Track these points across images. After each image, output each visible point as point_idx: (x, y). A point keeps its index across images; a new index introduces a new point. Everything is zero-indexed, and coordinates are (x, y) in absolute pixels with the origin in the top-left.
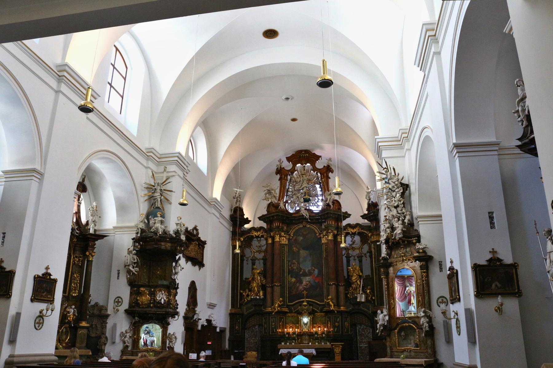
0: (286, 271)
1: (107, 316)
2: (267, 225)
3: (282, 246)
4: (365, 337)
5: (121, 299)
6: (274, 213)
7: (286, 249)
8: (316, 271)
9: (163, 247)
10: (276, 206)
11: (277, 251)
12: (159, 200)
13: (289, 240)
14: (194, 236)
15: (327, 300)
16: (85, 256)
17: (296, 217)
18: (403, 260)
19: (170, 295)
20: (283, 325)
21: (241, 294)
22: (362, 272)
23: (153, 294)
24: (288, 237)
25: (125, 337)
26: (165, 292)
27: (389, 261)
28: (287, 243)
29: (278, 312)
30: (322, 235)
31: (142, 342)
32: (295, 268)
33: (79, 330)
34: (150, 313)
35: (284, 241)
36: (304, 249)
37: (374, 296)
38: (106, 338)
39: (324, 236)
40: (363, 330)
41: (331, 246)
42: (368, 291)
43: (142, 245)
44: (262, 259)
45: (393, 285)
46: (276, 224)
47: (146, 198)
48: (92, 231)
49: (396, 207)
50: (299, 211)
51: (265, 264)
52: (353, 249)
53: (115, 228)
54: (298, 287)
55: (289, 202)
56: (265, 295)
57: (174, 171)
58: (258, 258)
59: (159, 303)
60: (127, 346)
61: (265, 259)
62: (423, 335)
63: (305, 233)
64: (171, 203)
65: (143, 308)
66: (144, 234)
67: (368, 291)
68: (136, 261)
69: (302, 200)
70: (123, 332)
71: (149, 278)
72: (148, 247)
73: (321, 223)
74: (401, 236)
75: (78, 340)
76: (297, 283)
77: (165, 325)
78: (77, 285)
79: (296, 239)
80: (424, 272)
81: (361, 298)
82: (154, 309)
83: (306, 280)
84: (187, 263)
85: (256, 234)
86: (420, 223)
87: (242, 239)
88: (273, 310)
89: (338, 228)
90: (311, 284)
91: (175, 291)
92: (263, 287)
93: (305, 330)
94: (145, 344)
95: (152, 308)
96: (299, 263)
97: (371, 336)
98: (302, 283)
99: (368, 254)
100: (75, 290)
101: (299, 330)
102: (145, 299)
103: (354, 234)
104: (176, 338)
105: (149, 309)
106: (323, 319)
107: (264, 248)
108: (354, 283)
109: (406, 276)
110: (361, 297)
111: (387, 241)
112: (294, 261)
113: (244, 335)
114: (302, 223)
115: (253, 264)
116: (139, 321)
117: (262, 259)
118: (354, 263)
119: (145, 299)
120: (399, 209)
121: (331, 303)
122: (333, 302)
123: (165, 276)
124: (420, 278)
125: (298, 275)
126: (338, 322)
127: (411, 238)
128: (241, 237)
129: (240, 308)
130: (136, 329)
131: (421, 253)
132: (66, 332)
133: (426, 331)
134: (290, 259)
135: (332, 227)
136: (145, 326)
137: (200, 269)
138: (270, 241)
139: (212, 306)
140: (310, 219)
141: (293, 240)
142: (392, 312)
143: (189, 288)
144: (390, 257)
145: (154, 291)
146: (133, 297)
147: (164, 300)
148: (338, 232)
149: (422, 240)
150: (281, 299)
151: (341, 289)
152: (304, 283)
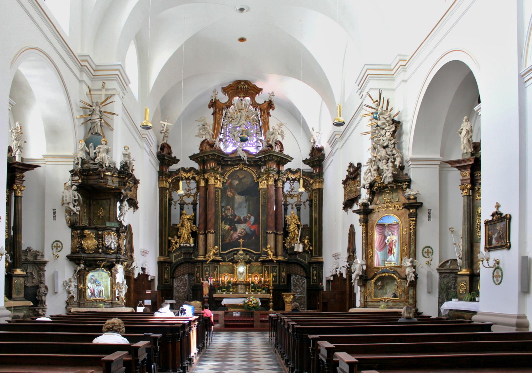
0: (219, 217)
2: (200, 165)
3: (217, 189)
4: (299, 287)
6: (209, 152)
7: (220, 192)
8: (252, 219)
10: (212, 145)
11: (212, 196)
13: (223, 183)
15: (267, 249)
17: (231, 158)
18: (387, 207)
20: (217, 274)
21: (169, 241)
22: (300, 221)
23: (100, 238)
24: (222, 179)
25: (69, 287)
27: (370, 207)
28: (221, 186)
29: (213, 261)
30: (260, 180)
31: (88, 292)
32: (229, 214)
35: (219, 185)
36: (240, 194)
37: (312, 246)
39: (262, 180)
40: (298, 280)
41: (272, 191)
42: (306, 241)
44: (192, 204)
45: (373, 233)
46: (211, 165)
49: (384, 147)
50: (235, 152)
51: (195, 210)
52: (292, 196)
54: (232, 234)
55: (223, 140)
56: (196, 242)
58: (187, 202)
60: (73, 297)
61: (194, 204)
62: (407, 285)
63: (241, 177)
65: (89, 253)
66: (86, 165)
67: (306, 241)
69: (239, 139)
70: (66, 281)
71: (90, 219)
73: (259, 167)
74: (391, 180)
76: (231, 230)
79: (230, 183)
80: (413, 221)
81: (299, 248)
82: (102, 255)
83: (241, 228)
85: (185, 175)
86: (411, 166)
87: (170, 180)
88: (207, 258)
89: (279, 172)
90: (247, 232)
92: (194, 234)
93: (241, 279)
94: (93, 294)
96: (233, 210)
97: (306, 286)
98: (236, 231)
99: (308, 202)
101: (234, 280)
103: (294, 180)
105: (97, 255)
106: (260, 268)
107: (194, 192)
108: (291, 232)
109: (386, 224)
110: (298, 247)
111: (372, 185)
112: (228, 207)
113: (173, 284)
114: (237, 165)
115: (182, 209)
116: (85, 269)
117: (192, 204)
118: (292, 212)
119: (90, 243)
120: (388, 150)
121: (270, 252)
122: (272, 252)
123: (109, 217)
124: (408, 226)
125: (233, 222)
126: (276, 272)
127: (401, 183)
128: (169, 178)
129: (168, 256)
130: (81, 277)
131: (413, 199)
133: (411, 282)
134: (223, 204)
135: (273, 170)
136: (90, 274)
137: (134, 212)
138: (202, 184)
139: (144, 253)
140: (248, 161)
141: (227, 184)
142: (369, 261)
144: (371, 204)
145: (102, 234)
146: (76, 241)
148: (279, 177)
149: (412, 186)
150: (217, 247)
151: (280, 238)
152: (239, 231)
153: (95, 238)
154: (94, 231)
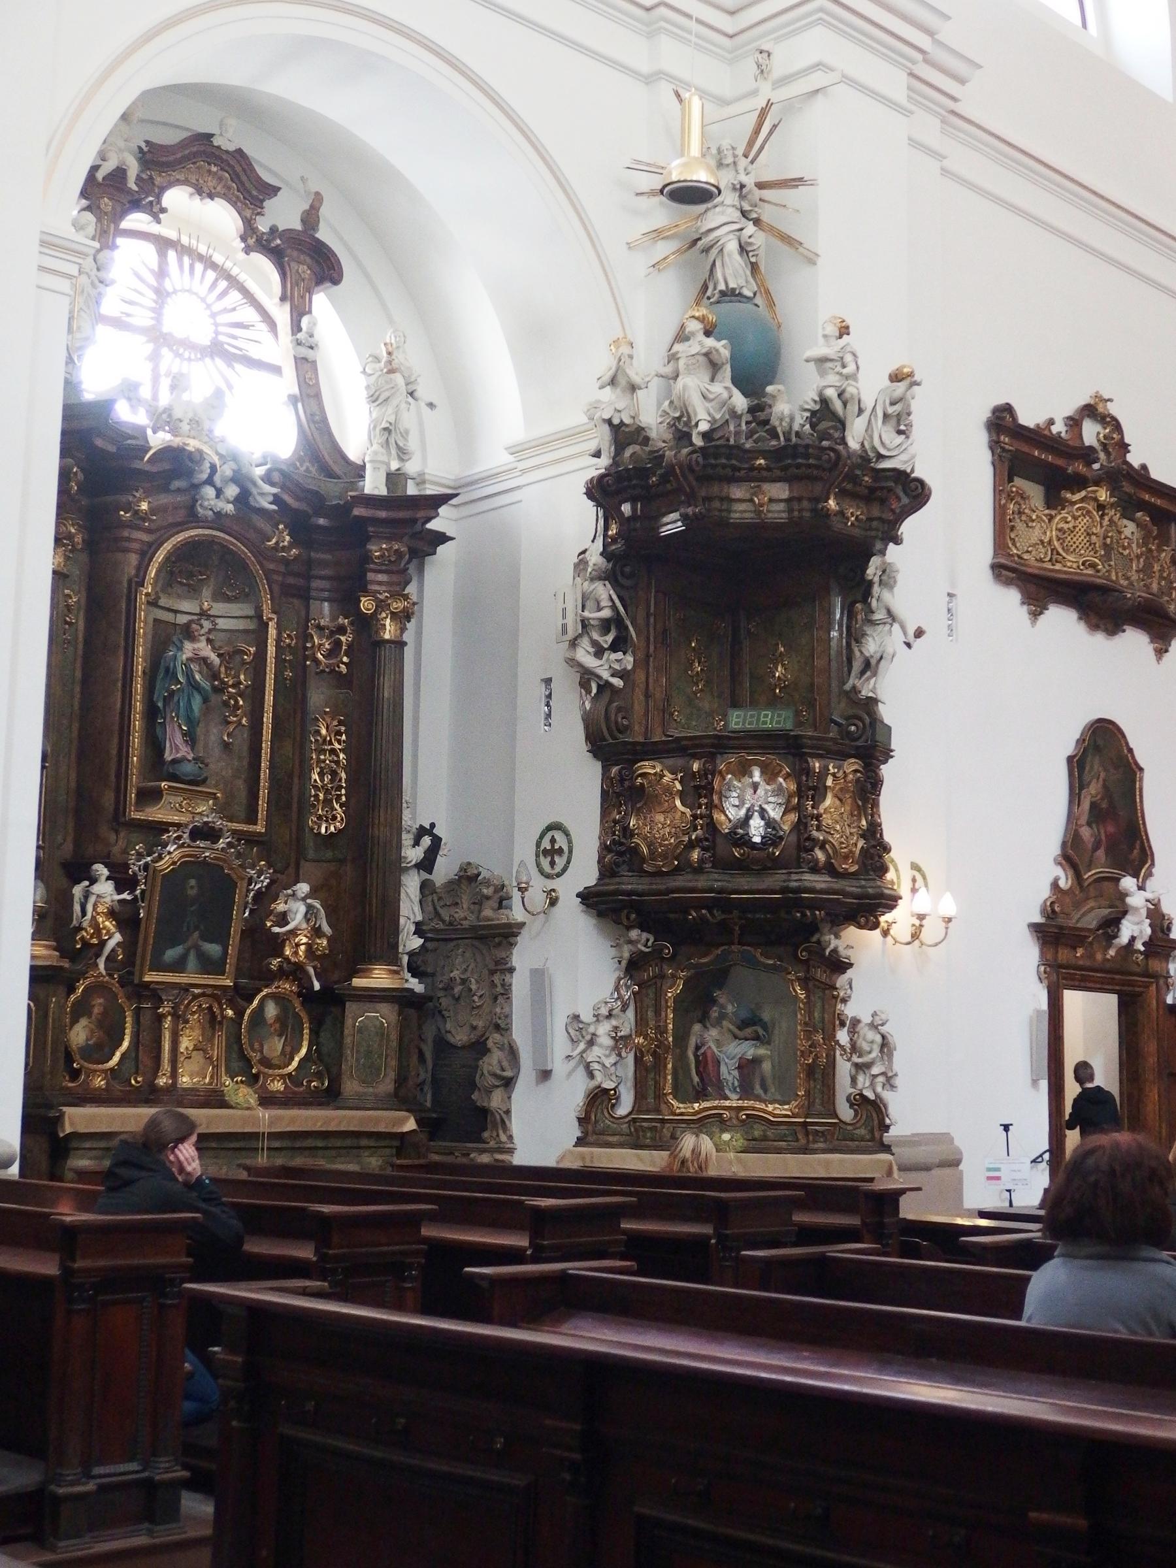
1: (508, 934)
5: (567, 834)
9: (741, 512)
12: (732, 246)
14: (1088, 455)
16: (366, 625)
19: (809, 790)
23: (702, 791)
25: (591, 1043)
26: (770, 775)
33: (351, 1007)
34: (700, 904)
38: (513, 1053)
43: (634, 517)
47: (664, 249)
48: (373, 484)
53: (516, 450)
57: (818, 66)
59: (744, 841)
64: (811, 260)
65: (659, 874)
68: (606, 613)
72: (672, 524)
75: (350, 1060)
77: (820, 974)
78: (334, 773)
82: (715, 880)
84: (1035, 615)
91: (851, 766)
95: (699, 870)
100: (327, 802)
102: (664, 824)
104: (885, 1045)
132: (282, 1020)
143: (1077, 765)
145: (709, 772)
147: (769, 823)
153: (682, 795)
154: (680, 762)
